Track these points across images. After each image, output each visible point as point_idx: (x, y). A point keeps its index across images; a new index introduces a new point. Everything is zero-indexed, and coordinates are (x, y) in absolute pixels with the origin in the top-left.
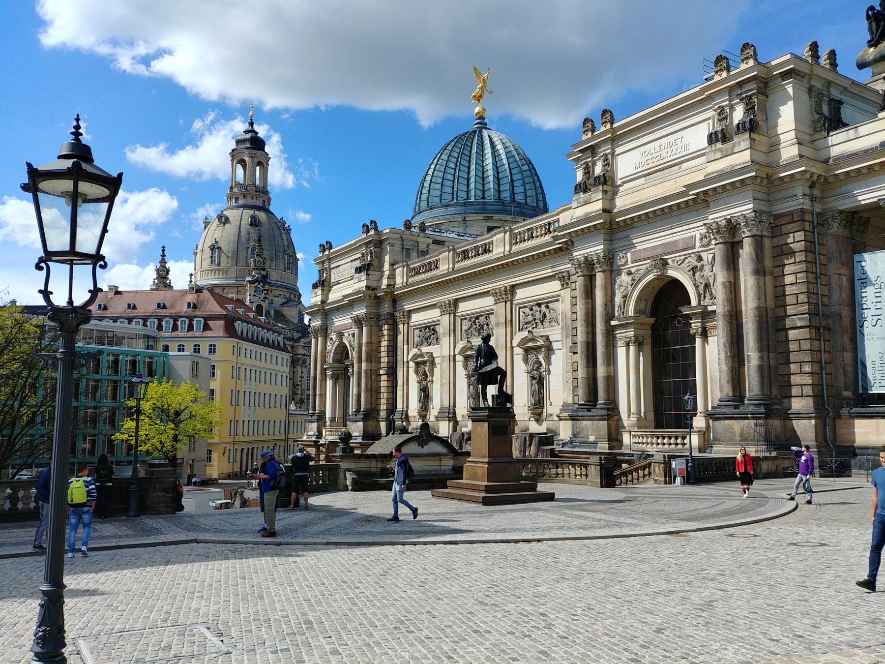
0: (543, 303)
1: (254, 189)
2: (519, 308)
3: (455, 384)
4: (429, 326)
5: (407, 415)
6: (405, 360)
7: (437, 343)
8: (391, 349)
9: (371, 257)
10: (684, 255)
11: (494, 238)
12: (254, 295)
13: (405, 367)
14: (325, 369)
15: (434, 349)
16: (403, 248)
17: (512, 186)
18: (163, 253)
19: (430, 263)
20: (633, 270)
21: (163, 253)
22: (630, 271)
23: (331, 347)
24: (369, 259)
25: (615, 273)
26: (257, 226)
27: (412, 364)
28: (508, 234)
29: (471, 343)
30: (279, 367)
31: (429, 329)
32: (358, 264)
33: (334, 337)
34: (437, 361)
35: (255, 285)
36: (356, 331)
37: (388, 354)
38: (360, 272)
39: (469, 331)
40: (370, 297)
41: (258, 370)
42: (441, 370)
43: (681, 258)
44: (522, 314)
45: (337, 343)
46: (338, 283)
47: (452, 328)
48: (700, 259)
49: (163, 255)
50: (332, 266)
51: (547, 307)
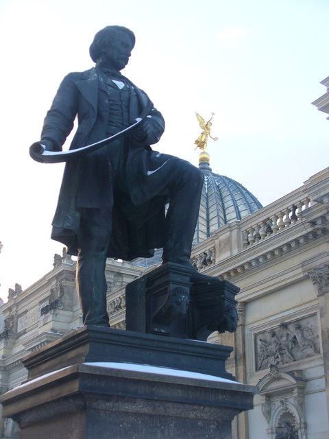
0: (290, 323)
2: (256, 335)
9: (62, 292)
11: (217, 242)
17: (236, 208)
28: (235, 232)
32: (47, 303)
44: (259, 343)
46: (24, 332)
50: (20, 312)
51: (299, 327)
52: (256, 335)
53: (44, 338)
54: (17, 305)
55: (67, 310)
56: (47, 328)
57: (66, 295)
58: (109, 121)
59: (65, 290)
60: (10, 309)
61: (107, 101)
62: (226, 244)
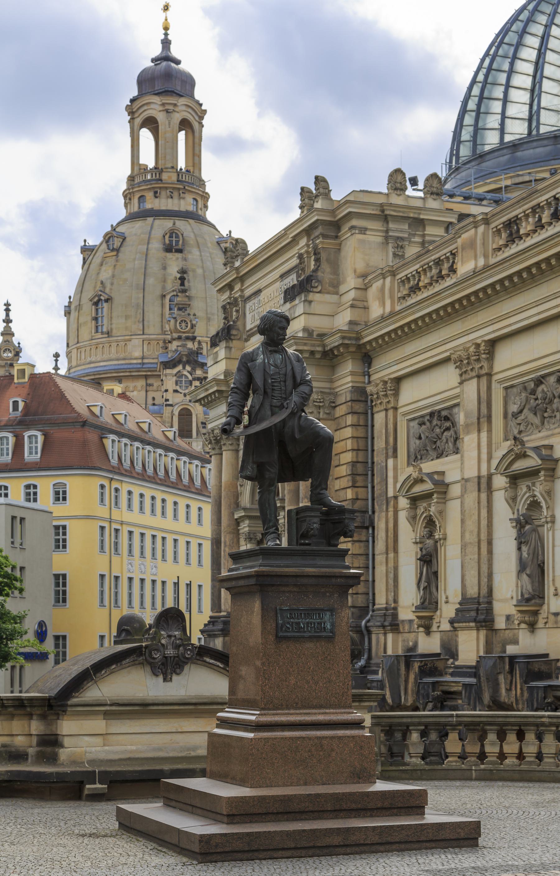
1: (174, 177)
3: (490, 543)
4: (439, 411)
5: (395, 616)
6: (391, 493)
7: (457, 451)
8: (360, 468)
12: (176, 391)
13: (391, 509)
14: (238, 522)
16: (387, 238)
18: (7, 315)
21: (7, 315)
24: (312, 267)
26: (180, 251)
27: (403, 502)
29: (522, 443)
30: (193, 528)
32: (292, 280)
34: (455, 491)
35: (175, 371)
37: (354, 481)
38: (292, 299)
39: (522, 417)
41: (159, 535)
42: (463, 512)
47: (484, 410)
49: (8, 321)
50: (248, 293)
54: (242, 279)
55: (328, 293)
57: (325, 266)
58: (272, 396)
59: (323, 256)
60: (230, 286)
61: (270, 381)
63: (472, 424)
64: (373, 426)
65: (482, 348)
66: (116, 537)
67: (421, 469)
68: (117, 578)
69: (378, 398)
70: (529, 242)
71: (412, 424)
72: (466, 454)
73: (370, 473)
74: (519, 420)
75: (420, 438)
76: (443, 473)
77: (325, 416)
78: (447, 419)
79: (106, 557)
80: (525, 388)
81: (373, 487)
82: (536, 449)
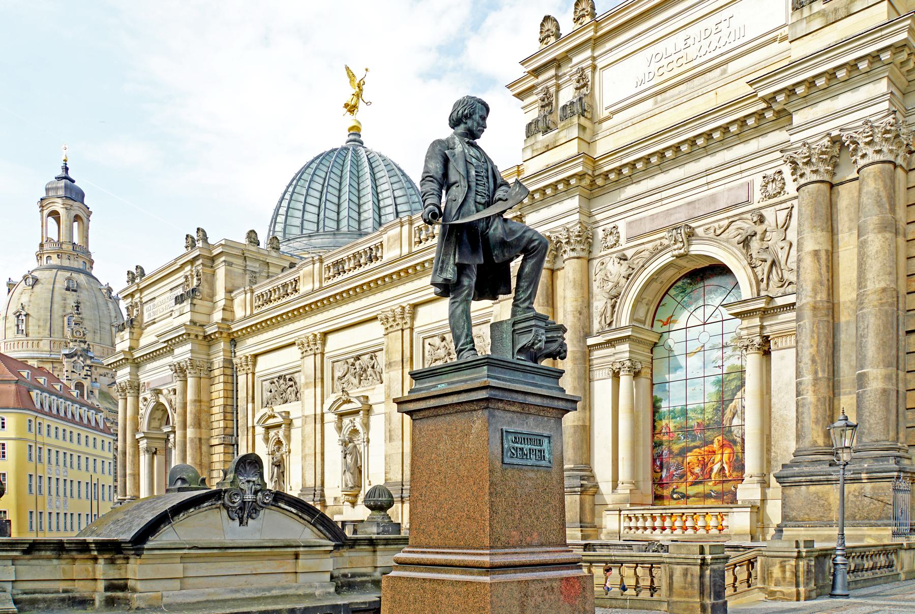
2: (424, 339)
6: (250, 425)
8: (229, 409)
10: (728, 218)
11: (385, 237)
15: (294, 409)
19: (285, 286)
20: (629, 253)
22: (624, 255)
23: (145, 411)
25: (595, 262)
29: (348, 394)
31: (285, 380)
33: (148, 396)
34: (297, 423)
36: (178, 385)
37: (225, 416)
39: (346, 378)
40: (197, 336)
42: (303, 436)
43: (721, 223)
45: (152, 404)
48: (762, 220)
52: (424, 339)
53: (182, 330)
56: (186, 318)
62: (395, 240)
63: (311, 382)
64: (237, 384)
65: (318, 336)
66: (40, 453)
67: (273, 410)
68: (40, 477)
69: (241, 366)
70: (351, 274)
71: (264, 383)
72: (306, 401)
73: (235, 412)
74: (343, 381)
75: (271, 392)
76: (288, 413)
77: (205, 376)
78: (290, 380)
79: (33, 464)
80: (347, 363)
81: (237, 421)
82: (357, 398)
